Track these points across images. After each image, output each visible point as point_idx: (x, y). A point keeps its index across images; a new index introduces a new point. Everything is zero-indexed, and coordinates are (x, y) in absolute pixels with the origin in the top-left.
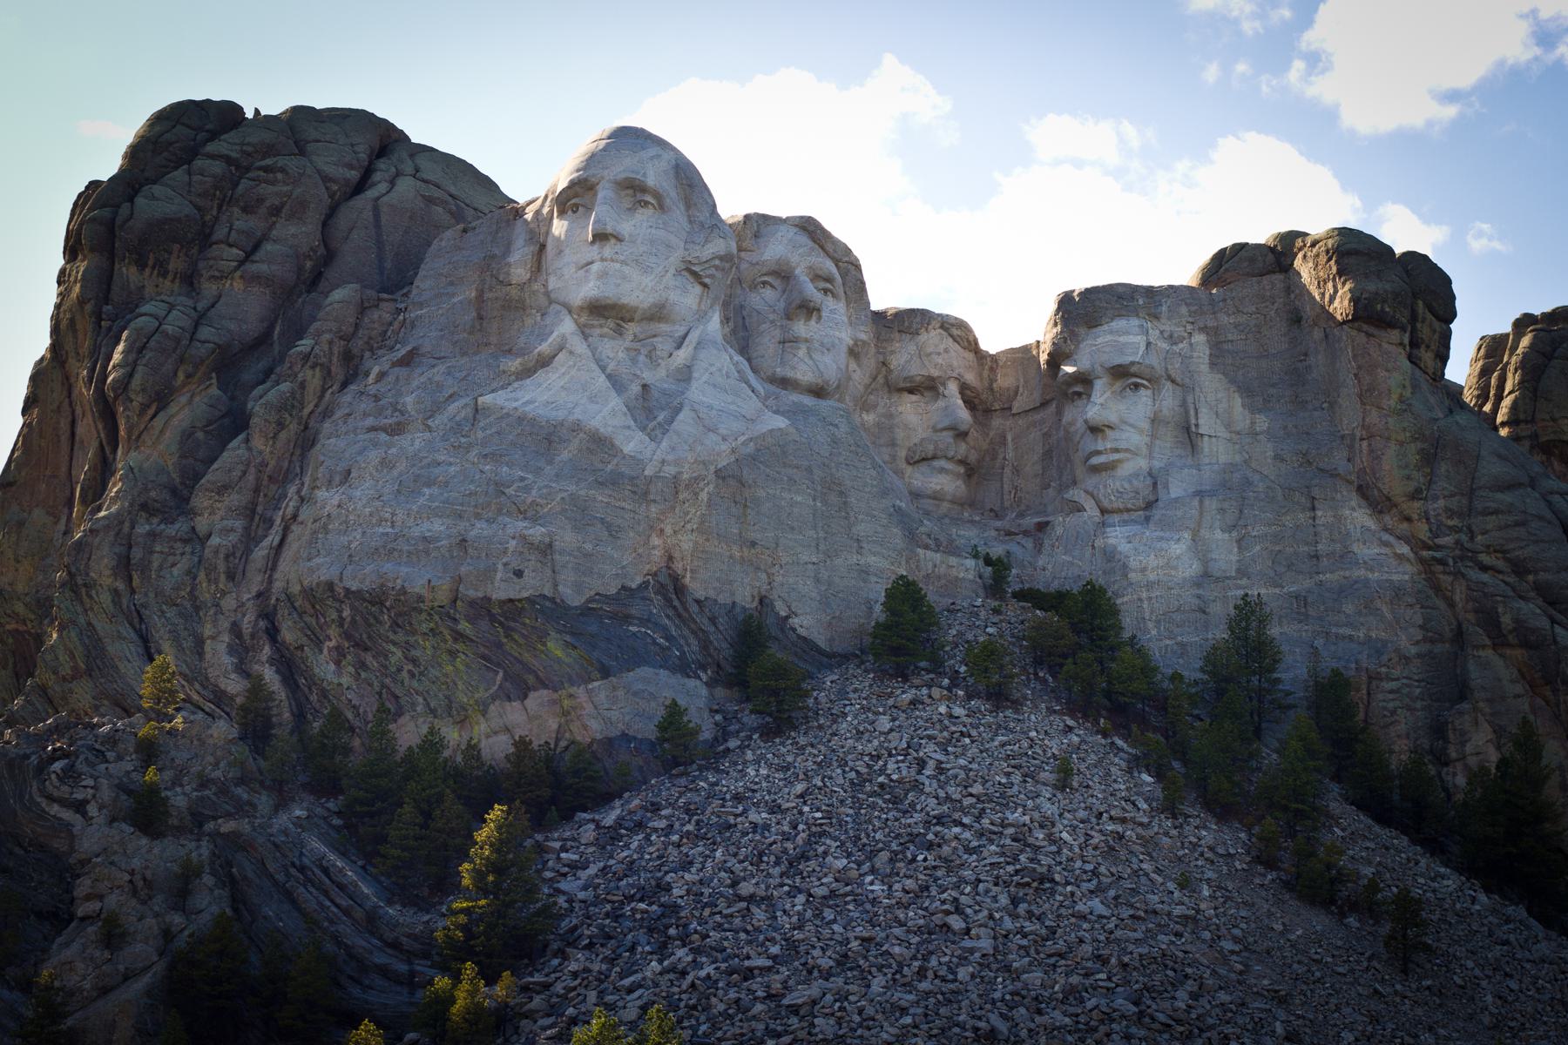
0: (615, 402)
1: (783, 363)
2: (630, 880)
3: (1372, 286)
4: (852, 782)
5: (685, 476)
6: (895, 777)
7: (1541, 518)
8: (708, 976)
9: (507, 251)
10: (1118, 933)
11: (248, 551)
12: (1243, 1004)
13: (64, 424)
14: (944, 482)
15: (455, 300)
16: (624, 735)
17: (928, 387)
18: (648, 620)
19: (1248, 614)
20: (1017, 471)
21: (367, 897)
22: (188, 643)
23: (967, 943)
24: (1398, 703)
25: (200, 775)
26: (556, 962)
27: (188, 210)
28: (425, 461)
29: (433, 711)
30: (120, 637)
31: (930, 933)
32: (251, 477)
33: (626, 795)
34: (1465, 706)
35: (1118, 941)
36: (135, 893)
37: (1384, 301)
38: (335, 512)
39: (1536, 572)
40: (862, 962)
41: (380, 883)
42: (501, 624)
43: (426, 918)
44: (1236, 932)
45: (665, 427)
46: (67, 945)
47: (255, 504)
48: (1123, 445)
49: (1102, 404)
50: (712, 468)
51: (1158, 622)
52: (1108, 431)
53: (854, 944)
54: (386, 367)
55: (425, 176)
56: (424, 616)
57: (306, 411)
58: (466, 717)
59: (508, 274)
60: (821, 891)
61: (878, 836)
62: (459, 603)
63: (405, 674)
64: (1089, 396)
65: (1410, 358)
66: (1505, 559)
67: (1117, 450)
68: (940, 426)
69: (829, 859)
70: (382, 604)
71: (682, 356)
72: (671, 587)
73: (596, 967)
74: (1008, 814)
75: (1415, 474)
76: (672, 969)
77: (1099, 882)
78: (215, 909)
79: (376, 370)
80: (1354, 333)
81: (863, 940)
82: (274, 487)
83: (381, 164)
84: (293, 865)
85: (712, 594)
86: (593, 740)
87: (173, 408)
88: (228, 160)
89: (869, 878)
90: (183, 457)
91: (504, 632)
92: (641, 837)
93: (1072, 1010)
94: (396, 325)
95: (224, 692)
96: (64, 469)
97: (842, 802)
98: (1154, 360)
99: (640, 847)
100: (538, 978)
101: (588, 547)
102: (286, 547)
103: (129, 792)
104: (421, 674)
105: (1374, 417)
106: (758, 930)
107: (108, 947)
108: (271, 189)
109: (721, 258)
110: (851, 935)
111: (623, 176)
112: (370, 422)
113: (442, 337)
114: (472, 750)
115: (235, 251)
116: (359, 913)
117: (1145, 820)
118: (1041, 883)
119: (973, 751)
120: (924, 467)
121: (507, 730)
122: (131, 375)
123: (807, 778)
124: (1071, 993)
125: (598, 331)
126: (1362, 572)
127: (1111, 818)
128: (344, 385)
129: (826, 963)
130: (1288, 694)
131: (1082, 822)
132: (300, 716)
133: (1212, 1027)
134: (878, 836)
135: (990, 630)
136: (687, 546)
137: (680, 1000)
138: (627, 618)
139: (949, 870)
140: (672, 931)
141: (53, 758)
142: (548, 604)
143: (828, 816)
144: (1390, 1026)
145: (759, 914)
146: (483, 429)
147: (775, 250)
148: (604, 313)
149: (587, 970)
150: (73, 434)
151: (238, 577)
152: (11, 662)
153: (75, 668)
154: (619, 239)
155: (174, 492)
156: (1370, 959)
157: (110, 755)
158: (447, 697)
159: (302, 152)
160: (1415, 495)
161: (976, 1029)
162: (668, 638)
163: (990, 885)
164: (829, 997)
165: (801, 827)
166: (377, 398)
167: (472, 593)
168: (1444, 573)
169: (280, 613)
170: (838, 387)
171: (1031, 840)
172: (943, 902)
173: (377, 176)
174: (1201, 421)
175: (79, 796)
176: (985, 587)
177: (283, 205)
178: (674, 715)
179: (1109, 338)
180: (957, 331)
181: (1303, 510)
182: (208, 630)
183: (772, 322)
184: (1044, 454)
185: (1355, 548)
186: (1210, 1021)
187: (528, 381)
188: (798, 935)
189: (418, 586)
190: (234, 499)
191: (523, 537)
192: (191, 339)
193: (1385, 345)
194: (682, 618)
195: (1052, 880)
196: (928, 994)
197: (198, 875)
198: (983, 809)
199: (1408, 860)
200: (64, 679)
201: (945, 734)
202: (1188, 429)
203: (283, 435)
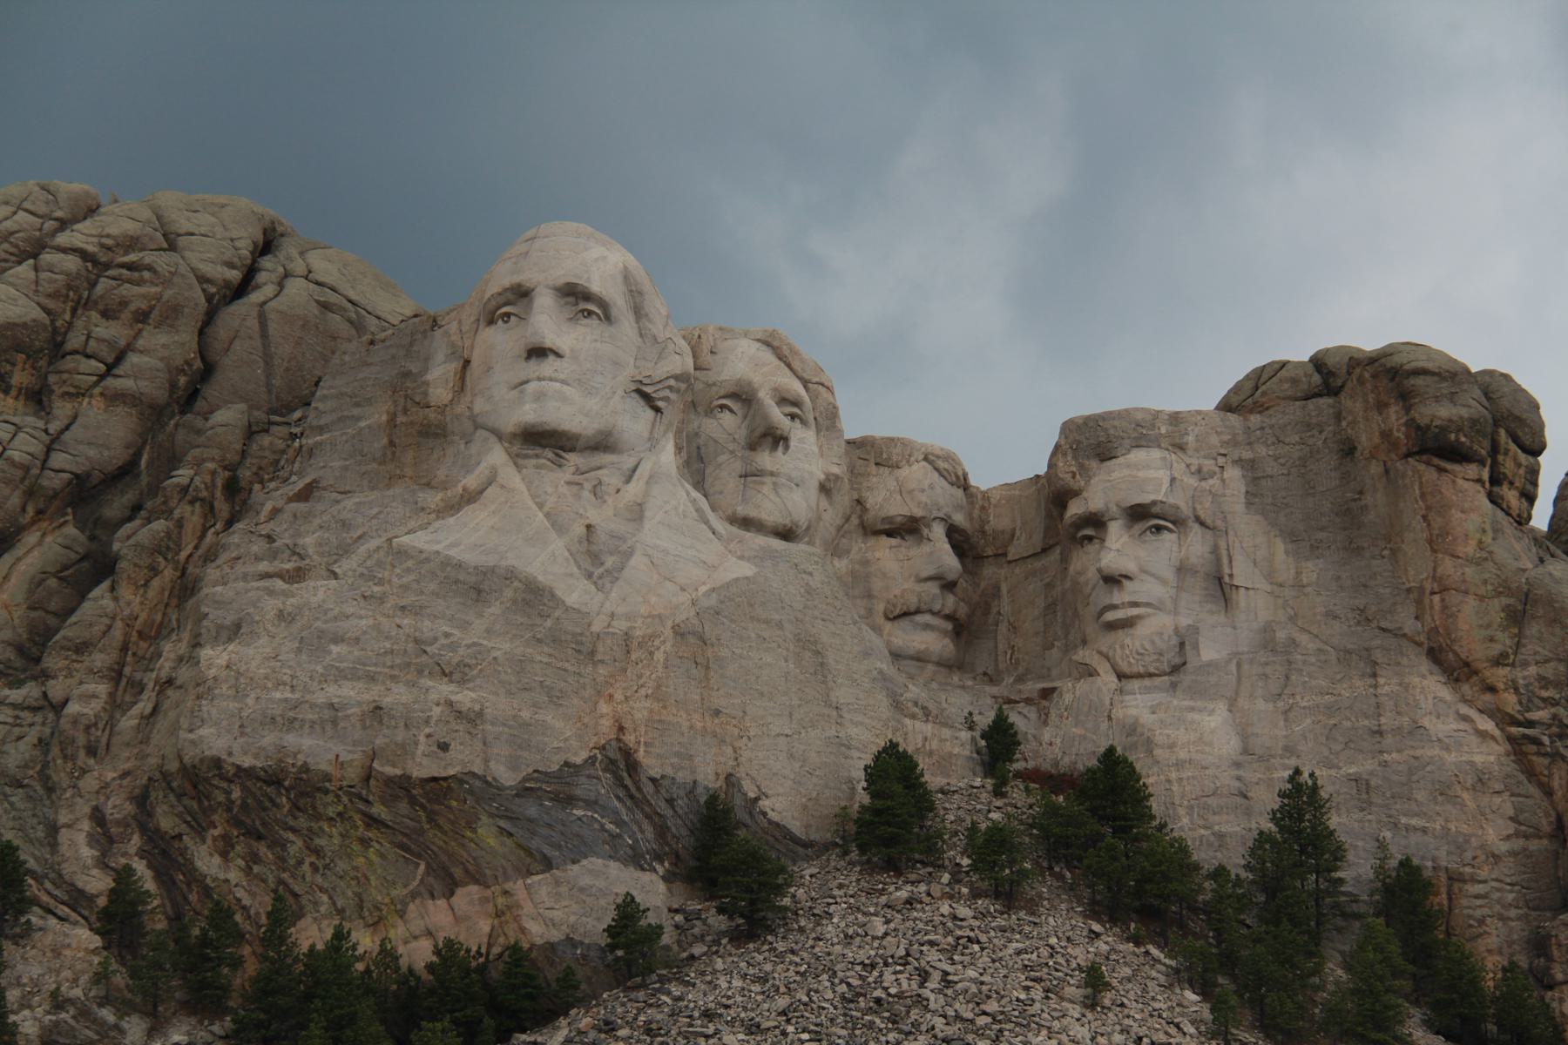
0: (558, 545)
1: (745, 500)
4: (843, 998)
6: (893, 991)
11: (111, 723)
14: (930, 640)
15: (363, 424)
16: (569, 939)
17: (907, 529)
18: (596, 802)
19: (1301, 803)
20: (1013, 628)
24: (1486, 911)
25: (55, 994)
28: (330, 615)
32: (118, 632)
33: (573, 1012)
37: (1459, 430)
42: (423, 807)
45: (614, 575)
47: (122, 664)
49: (1118, 548)
50: (669, 624)
51: (1191, 808)
52: (1126, 582)
55: (321, 279)
57: (183, 555)
58: (380, 919)
59: (426, 394)
62: (372, 782)
63: (306, 867)
67: (1135, 604)
68: (925, 574)
71: (634, 490)
72: (621, 762)
75: (1499, 635)
79: (269, 506)
80: (1422, 467)
83: (267, 262)
85: (669, 771)
87: (19, 551)
88: (83, 255)
91: (428, 816)
94: (291, 452)
95: (81, 892)
97: (832, 1020)
98: (1180, 500)
104: (326, 867)
108: (136, 290)
109: (676, 377)
111: (562, 281)
112: (264, 566)
113: (346, 468)
114: (387, 955)
115: (93, 363)
120: (905, 622)
121: (429, 933)
125: (534, 461)
126: (1437, 751)
128: (229, 523)
132: (176, 918)
135: (994, 816)
142: (478, 783)
148: (542, 441)
154: (558, 355)
155: (20, 650)
158: (356, 894)
159: (172, 247)
160: (1499, 661)
162: (619, 823)
166: (270, 538)
167: (389, 770)
168: (1539, 754)
169: (153, 795)
170: (808, 528)
173: (261, 277)
174: (1235, 571)
176: (983, 763)
177: (152, 308)
178: (628, 911)
179: (1126, 472)
181: (1363, 675)
182: (63, 818)
183: (732, 452)
184: (1048, 607)
185: (1426, 722)
187: (451, 520)
189: (322, 763)
190: (100, 659)
191: (450, 704)
192: (43, 468)
193: (1460, 481)
194: (635, 800)
198: (1001, 1031)
201: (950, 939)
202: (1220, 580)
203: (156, 583)
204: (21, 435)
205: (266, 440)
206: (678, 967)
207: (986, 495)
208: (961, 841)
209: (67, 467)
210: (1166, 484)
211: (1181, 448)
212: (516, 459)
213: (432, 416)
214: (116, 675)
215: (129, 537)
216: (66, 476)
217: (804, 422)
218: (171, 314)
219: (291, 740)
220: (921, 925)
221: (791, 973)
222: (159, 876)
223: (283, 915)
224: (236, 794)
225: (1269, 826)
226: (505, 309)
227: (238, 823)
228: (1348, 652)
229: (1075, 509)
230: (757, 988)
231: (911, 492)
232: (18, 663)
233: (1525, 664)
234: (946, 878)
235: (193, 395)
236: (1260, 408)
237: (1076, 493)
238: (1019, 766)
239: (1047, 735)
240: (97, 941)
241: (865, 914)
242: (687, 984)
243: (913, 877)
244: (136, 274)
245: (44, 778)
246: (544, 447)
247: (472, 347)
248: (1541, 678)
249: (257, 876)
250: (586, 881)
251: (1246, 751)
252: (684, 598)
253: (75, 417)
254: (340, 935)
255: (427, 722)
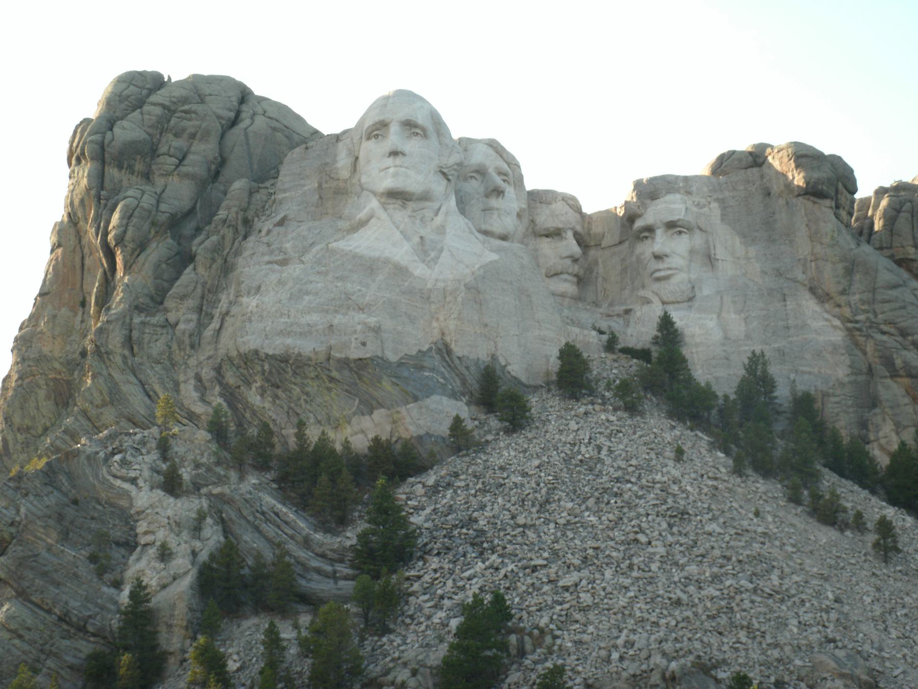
0: (407, 246)
2: (453, 516)
3: (816, 175)
5: (449, 288)
7: (913, 304)
8: (512, 571)
9: (335, 161)
10: (732, 543)
11: (200, 334)
12: (806, 582)
13: (78, 260)
14: (567, 286)
15: (306, 188)
16: (427, 434)
17: (555, 234)
19: (756, 362)
20: (605, 280)
21: (303, 529)
22: (170, 385)
23: (650, 550)
24: (839, 410)
26: (421, 563)
27: (144, 136)
29: (319, 422)
30: (129, 382)
31: (629, 544)
32: (199, 290)
33: (435, 468)
34: (877, 410)
35: (732, 547)
36: (172, 530)
37: (823, 184)
38: (255, 310)
39: (913, 335)
40: (596, 561)
41: (307, 520)
42: (356, 373)
43: (339, 539)
44: (792, 541)
46: (138, 560)
48: (673, 266)
49: (661, 242)
53: (590, 552)
54: (271, 227)
55: (271, 115)
56: (311, 369)
57: (225, 252)
60: (562, 521)
61: (586, 489)
62: (331, 361)
63: (302, 401)
64: (653, 239)
65: (835, 214)
66: (896, 328)
67: (670, 269)
68: (564, 255)
69: (562, 503)
70: (287, 361)
71: (439, 219)
72: (444, 350)
73: (446, 566)
74: (654, 476)
76: (491, 567)
77: (713, 515)
78: (215, 537)
80: (806, 201)
81: (595, 549)
82: (211, 296)
83: (244, 108)
84: (257, 511)
85: (466, 353)
86: (412, 437)
87: (148, 251)
88: (164, 106)
89: (587, 514)
90: (156, 278)
91: (359, 376)
92: (451, 491)
93: (718, 587)
94: (270, 202)
95: (193, 413)
96: (78, 285)
97: (561, 470)
98: (689, 218)
99: (452, 498)
100: (412, 573)
101: (399, 328)
102: (223, 331)
103: (158, 472)
104: (311, 401)
105: (818, 249)
106: (532, 543)
107: (162, 561)
108: (191, 123)
109: (458, 164)
110: (585, 546)
111: (404, 118)
112: (267, 258)
114: (346, 444)
115: (174, 159)
116: (299, 538)
117: (726, 478)
118: (682, 514)
119: (625, 441)
120: (555, 279)
121: (363, 432)
122: (125, 232)
123: (538, 457)
124: (716, 578)
125: (392, 206)
127: (709, 478)
128: (245, 238)
129: (577, 562)
130: (780, 405)
131: (695, 480)
132: (240, 425)
133: (793, 596)
134: (586, 489)
135: (614, 371)
136: (452, 327)
137: (500, 584)
138: (422, 368)
139: (630, 508)
140: (485, 545)
141: (113, 454)
142: (380, 361)
143: (556, 478)
144: (887, 593)
145: (531, 534)
146: (334, 262)
147: (478, 157)
148: (397, 196)
149: (441, 568)
150: (83, 265)
151: (197, 347)
152: (53, 396)
153: (103, 400)
154: (404, 154)
155: (152, 298)
156: (865, 555)
157: (144, 451)
158: (327, 414)
159: (202, 101)
160: (843, 292)
161: (670, 599)
162: (445, 378)
163: (655, 517)
164: (584, 582)
165: (542, 485)
166: (268, 245)
167: (338, 355)
168: (861, 336)
169: (224, 368)
171: (670, 491)
172: (633, 527)
173: (243, 115)
174: (718, 252)
175: (132, 474)
176: (603, 346)
177: (197, 132)
178: (458, 421)
180: (573, 204)
182: (182, 378)
185: (809, 322)
186: (793, 592)
187: (355, 235)
188: (557, 546)
190: (191, 303)
191: (365, 324)
192: (157, 210)
193: (823, 208)
194: (451, 367)
195: (688, 513)
196: (637, 579)
197: (205, 518)
199: (865, 498)
200: (97, 407)
201: (608, 431)
202: (709, 257)
203: (214, 266)
204: (146, 196)
205: (258, 196)
206: (481, 447)
207: (590, 217)
208: (602, 384)
209: (167, 210)
210: (683, 213)
211: (689, 193)
212: (384, 206)
213: (341, 184)
214: (200, 310)
215: (200, 244)
216: (167, 215)
217: (509, 183)
218: (207, 134)
219: (289, 341)
220: (593, 425)
221: (537, 448)
222: (230, 405)
223: (301, 425)
224: (267, 367)
225: (743, 372)
226: (375, 133)
227: (268, 380)
228: (772, 290)
229: (639, 224)
230: (521, 455)
231: (557, 216)
232: (152, 305)
233: (854, 294)
234: (600, 401)
235: (217, 173)
236: (724, 173)
237: (639, 216)
238: (619, 347)
239: (629, 331)
240: (209, 436)
241: (566, 420)
242: (488, 454)
243: (585, 402)
244: (188, 116)
245: (170, 359)
246: (397, 199)
247: (359, 151)
248: (861, 300)
249: (279, 405)
250: (433, 406)
251: (726, 338)
252: (468, 271)
253: (166, 186)
254: (323, 433)
255: (355, 332)
